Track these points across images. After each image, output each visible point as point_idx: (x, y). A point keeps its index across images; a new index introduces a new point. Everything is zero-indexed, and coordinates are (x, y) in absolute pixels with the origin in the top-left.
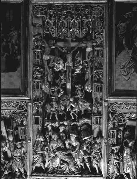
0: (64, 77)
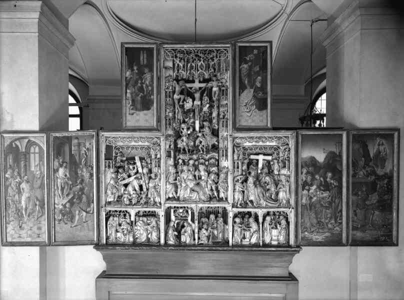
0: (193, 116)
